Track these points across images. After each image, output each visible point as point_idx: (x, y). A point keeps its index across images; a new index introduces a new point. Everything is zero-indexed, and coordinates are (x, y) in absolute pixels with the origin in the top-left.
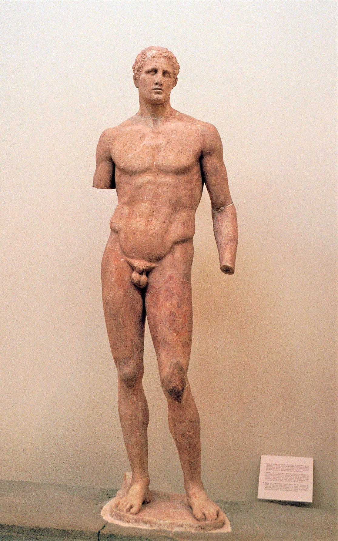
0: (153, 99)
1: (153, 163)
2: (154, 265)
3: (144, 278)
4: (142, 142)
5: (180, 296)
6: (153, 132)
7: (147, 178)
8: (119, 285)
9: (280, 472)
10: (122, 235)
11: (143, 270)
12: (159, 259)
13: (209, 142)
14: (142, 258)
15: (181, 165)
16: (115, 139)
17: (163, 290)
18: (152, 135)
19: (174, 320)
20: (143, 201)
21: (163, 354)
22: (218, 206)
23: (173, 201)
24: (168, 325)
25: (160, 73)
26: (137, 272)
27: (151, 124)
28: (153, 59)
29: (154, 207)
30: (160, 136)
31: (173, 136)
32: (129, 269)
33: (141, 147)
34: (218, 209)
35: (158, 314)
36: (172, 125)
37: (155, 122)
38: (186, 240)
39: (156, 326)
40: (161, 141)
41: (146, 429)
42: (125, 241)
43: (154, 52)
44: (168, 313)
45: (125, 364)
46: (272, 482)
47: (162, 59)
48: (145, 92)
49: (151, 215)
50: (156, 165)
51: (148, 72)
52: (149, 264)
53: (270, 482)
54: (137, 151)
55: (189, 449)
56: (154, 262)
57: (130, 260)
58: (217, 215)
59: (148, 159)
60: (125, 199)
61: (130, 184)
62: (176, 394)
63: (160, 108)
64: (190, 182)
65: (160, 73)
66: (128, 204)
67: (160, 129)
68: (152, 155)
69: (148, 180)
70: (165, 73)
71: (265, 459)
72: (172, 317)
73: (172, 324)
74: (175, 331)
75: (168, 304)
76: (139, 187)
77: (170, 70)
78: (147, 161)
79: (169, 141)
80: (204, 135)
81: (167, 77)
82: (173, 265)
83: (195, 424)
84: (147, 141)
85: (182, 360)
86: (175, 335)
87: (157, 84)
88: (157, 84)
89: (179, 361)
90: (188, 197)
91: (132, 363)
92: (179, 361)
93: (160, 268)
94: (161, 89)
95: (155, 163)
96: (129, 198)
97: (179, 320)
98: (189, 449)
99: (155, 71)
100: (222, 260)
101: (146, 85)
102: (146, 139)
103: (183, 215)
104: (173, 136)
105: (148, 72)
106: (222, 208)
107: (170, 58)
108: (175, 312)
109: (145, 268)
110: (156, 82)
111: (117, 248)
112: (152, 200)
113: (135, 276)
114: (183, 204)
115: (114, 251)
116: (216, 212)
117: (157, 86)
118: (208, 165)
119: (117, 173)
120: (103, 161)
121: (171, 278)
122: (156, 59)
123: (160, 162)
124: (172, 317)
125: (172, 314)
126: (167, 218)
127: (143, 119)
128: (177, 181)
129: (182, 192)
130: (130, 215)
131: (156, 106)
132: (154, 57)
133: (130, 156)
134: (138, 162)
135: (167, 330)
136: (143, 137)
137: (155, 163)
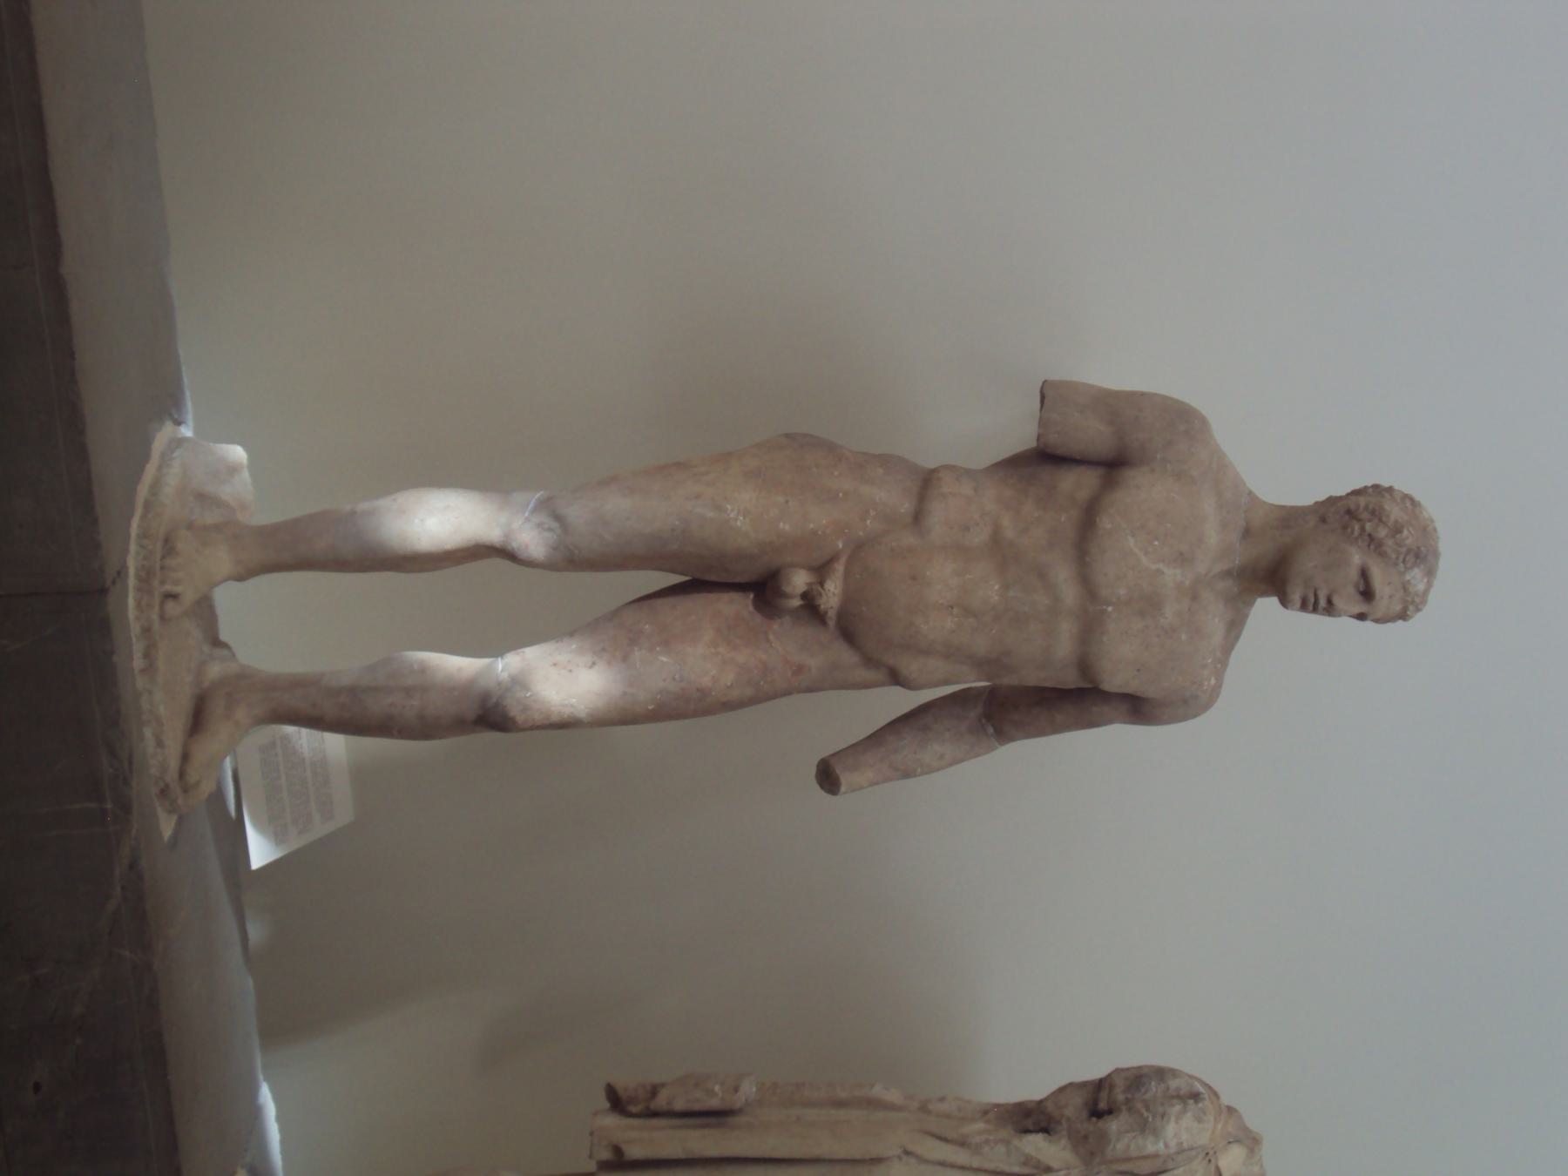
2: (832, 623)
3: (797, 602)
7: (1069, 593)
10: (909, 539)
12: (848, 634)
18: (1187, 583)
20: (1006, 587)
26: (810, 584)
27: (1218, 568)
31: (1184, 637)
33: (1154, 567)
36: (1214, 620)
37: (1227, 574)
40: (1170, 612)
49: (968, 611)
50: (1104, 612)
51: (1364, 574)
52: (832, 614)
54: (1144, 560)
57: (840, 567)
59: (1122, 592)
84: (1172, 575)
87: (1329, 602)
102: (1178, 572)
106: (991, 730)
107: (1403, 616)
110: (1336, 600)
133: (1131, 541)
136: (1183, 559)
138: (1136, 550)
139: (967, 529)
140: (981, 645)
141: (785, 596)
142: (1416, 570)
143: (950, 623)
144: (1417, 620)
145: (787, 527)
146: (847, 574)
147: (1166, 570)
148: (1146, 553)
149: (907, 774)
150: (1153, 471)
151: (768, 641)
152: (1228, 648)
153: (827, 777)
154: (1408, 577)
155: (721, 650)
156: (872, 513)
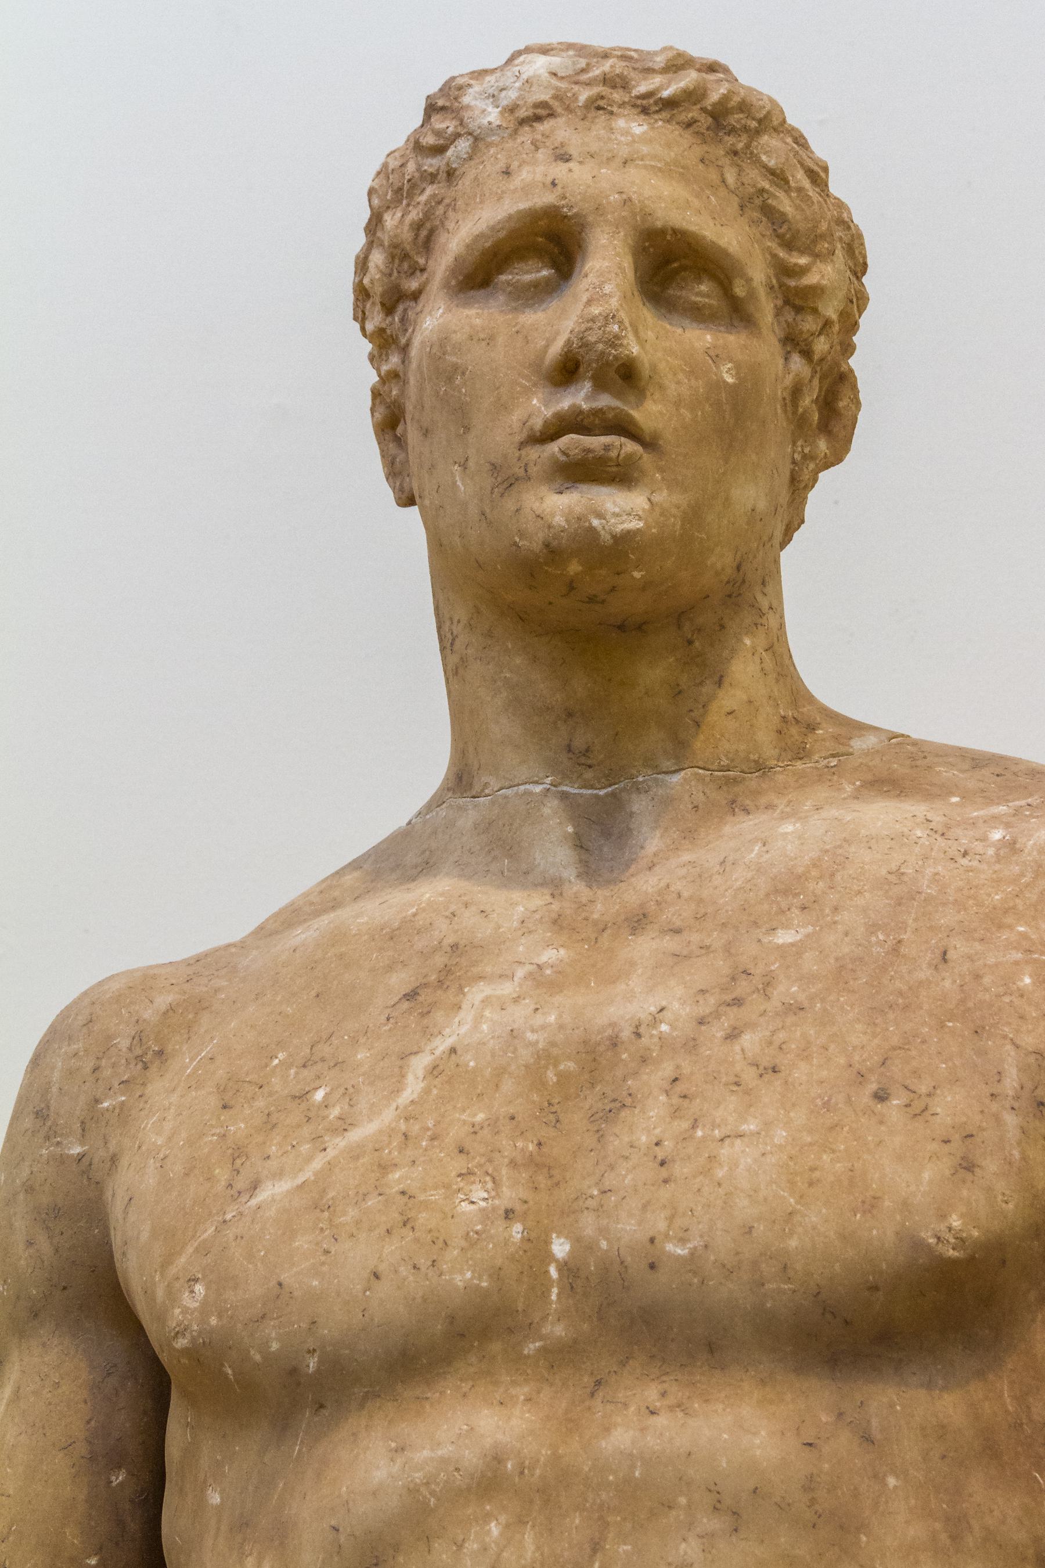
1: (537, 1248)
4: (429, 1033)
7: (475, 1424)
15: (882, 1232)
18: (549, 956)
25: (607, 267)
27: (553, 847)
28: (526, 135)
30: (645, 947)
31: (784, 937)
33: (413, 1087)
36: (788, 831)
40: (648, 995)
47: (638, 127)
50: (564, 1267)
51: (479, 276)
63: (653, 674)
65: (607, 267)
68: (540, 1166)
69: (471, 1458)
77: (729, 234)
78: (467, 1222)
79: (736, 992)
81: (698, 315)
87: (567, 371)
94: (624, 428)
95: (560, 1248)
99: (550, 244)
101: (461, 416)
102: (476, 994)
104: (784, 937)
105: (479, 276)
117: (579, 398)
122: (560, 130)
123: (628, 1228)
128: (844, 1442)
132: (542, 113)
133: (263, 1195)
134: (358, 1255)
137: (560, 1248)
147: (441, 1045)
148: (344, 1125)
154: (493, 116)
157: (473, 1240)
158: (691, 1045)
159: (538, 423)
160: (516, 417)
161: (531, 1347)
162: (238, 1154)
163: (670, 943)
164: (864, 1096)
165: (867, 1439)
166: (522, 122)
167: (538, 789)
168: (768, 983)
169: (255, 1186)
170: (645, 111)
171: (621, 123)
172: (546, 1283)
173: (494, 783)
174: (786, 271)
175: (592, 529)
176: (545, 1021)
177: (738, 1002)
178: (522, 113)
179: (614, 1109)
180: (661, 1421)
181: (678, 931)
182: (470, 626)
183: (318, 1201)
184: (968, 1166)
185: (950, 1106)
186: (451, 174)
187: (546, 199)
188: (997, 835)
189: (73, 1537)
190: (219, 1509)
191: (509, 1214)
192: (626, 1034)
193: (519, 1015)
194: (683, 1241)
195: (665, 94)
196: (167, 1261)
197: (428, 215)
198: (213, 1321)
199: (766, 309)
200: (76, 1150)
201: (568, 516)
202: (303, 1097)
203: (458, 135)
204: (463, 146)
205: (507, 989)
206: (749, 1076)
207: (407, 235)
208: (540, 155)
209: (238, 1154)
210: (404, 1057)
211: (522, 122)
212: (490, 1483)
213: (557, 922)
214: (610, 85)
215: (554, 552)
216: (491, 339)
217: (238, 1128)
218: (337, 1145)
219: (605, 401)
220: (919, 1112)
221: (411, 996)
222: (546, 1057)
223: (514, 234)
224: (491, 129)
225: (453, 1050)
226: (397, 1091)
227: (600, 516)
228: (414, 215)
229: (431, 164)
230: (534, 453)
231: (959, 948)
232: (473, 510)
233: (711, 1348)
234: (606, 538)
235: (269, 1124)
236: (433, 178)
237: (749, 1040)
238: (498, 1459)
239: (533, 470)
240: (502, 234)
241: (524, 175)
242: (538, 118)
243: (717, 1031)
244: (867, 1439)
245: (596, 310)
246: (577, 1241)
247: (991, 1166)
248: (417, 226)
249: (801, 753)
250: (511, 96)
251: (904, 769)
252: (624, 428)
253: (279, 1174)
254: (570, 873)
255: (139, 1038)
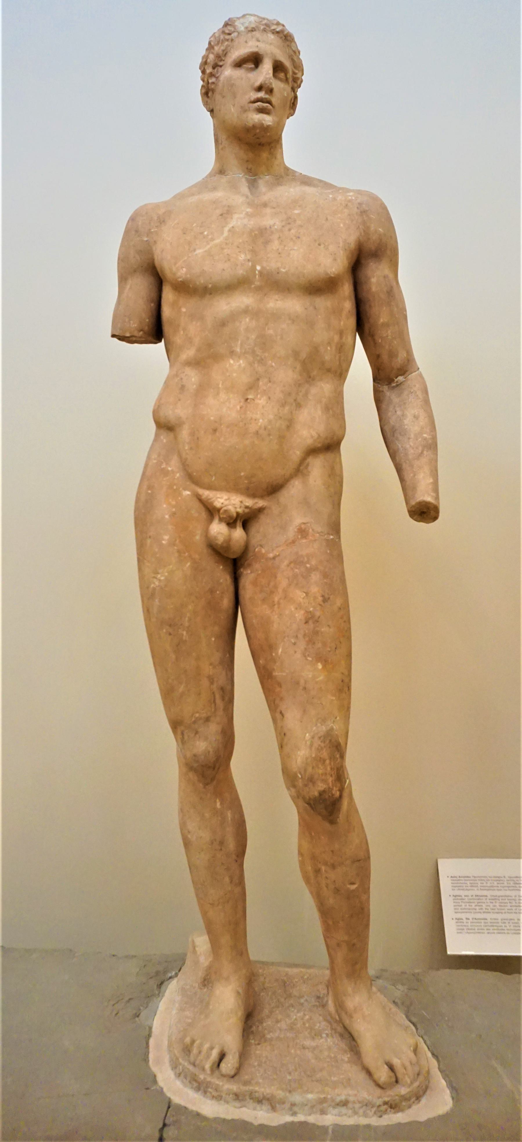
0: (250, 124)
1: (253, 268)
2: (261, 503)
3: (238, 533)
5: (325, 575)
6: (250, 204)
8: (179, 551)
9: (479, 893)
10: (184, 433)
11: (238, 514)
12: (273, 489)
13: (377, 229)
14: (234, 488)
15: (321, 270)
16: (162, 221)
17: (286, 563)
18: (249, 210)
19: (316, 633)
20: (232, 353)
21: (292, 718)
22: (389, 375)
23: (303, 355)
24: (302, 644)
25: (267, 67)
26: (221, 520)
27: (244, 188)
28: (250, 35)
29: (260, 369)
30: (268, 211)
31: (296, 212)
32: (204, 515)
33: (226, 234)
34: (390, 381)
35: (275, 618)
37: (253, 184)
38: (330, 446)
39: (272, 647)
41: (241, 865)
42: (191, 449)
43: (252, 19)
44: (300, 615)
45: (197, 733)
46: (468, 915)
47: (272, 36)
48: (232, 112)
50: (259, 271)
51: (239, 64)
52: (249, 502)
53: (463, 916)
54: (217, 241)
55: (346, 916)
56: (262, 497)
57: (206, 494)
58: (388, 394)
59: (242, 257)
60: (189, 353)
61: (202, 318)
62: (325, 807)
63: (265, 155)
64: (337, 312)
65: (267, 67)
66: (196, 363)
67: (265, 198)
68: (253, 251)
69: (243, 306)
70: (278, 67)
71: (449, 869)
72: (311, 625)
73: (311, 642)
74: (319, 658)
75: (299, 595)
76: (223, 323)
77: (287, 64)
79: (289, 221)
80: (363, 212)
81: (281, 80)
82: (305, 502)
83: (362, 863)
84: (237, 221)
85: (337, 727)
86: (320, 666)
87: (260, 89)
88: (260, 89)
89: (332, 729)
90: (334, 348)
91: (213, 728)
92: (332, 729)
93: (275, 510)
94: (269, 102)
95: (258, 268)
96: (199, 350)
97: (327, 630)
98: (346, 916)
99: (255, 60)
100: (414, 488)
102: (236, 216)
103: (325, 387)
104: (296, 212)
105: (239, 64)
106: (401, 378)
107: (287, 38)
108: (318, 614)
109: (240, 510)
110: (257, 84)
111: (173, 465)
112: (253, 352)
113: (218, 529)
114: (323, 363)
115: (165, 473)
116: (385, 388)
117: (261, 95)
118: (374, 280)
119: (168, 295)
120: (135, 271)
121: (302, 532)
122: (257, 34)
124: (311, 625)
125: (310, 618)
126: (290, 394)
127: (224, 179)
129: (321, 334)
130: (202, 389)
131: (253, 146)
132: (253, 30)
133: (198, 251)
134: (220, 266)
135: (298, 655)
136: (227, 213)
137: (258, 268)
138: (208, 247)
139: (183, 387)
140: (286, 375)
141: (228, 540)
142: (236, 24)
143: (262, 401)
144: (290, 28)
145: (166, 537)
146: (210, 488)
147: (230, 226)
148: (212, 239)
149: (432, 446)
150: (155, 242)
151: (274, 558)
152: (327, 185)
153: (425, 513)
154: (242, 29)
155: (276, 599)
156: (164, 466)
157: (242, 265)
158: (281, 231)
159: (252, 99)
160: (247, 97)
161: (253, 286)
162: (189, 243)
163: (273, 210)
164: (317, 244)
165: (315, 308)
166: (249, 31)
167: (241, 176)
168: (295, 221)
169: (195, 250)
170: (273, 33)
171: (269, 35)
172: (255, 275)
173: (231, 173)
174: (294, 73)
175: (263, 124)
176: (251, 223)
177: (289, 224)
178: (250, 29)
179: (267, 242)
180: (279, 302)
181: (274, 208)
182: (226, 139)
183: (209, 254)
184: (335, 260)
185: (332, 248)
186: (232, 40)
187: (255, 50)
188: (331, 196)
189: (144, 316)
190: (185, 312)
191: (249, 260)
192: (268, 227)
193: (245, 221)
194: (284, 269)
195: (278, 30)
196: (175, 264)
197: (226, 49)
198: (188, 276)
199: (290, 80)
200: (146, 239)
201: (259, 120)
202: (202, 233)
203: (234, 32)
204: (235, 34)
205: (242, 216)
206: (294, 238)
207: (221, 52)
208: (254, 39)
209: (189, 243)
210: (223, 227)
211: (249, 31)
212: (246, 311)
213: (249, 204)
214: (267, 27)
215: (254, 127)
216: (242, 79)
217: (188, 238)
218: (212, 244)
219: (267, 96)
220: (326, 248)
221: (222, 215)
222: (252, 231)
223: (249, 56)
224: (242, 31)
225: (233, 227)
226: (222, 233)
227: (264, 120)
228: (222, 48)
229: (227, 37)
230: (251, 105)
231: (329, 218)
232: (236, 115)
233: (288, 289)
234: (265, 126)
235: (195, 238)
236: (228, 40)
237: (293, 231)
238: (247, 306)
239: (251, 109)
240: (246, 56)
241: (250, 43)
242: (252, 31)
243: (286, 228)
244: (315, 308)
245: (268, 76)
246: (262, 267)
247: (339, 261)
248: (223, 51)
249: (288, 175)
250: (247, 25)
251: (306, 181)
252: (269, 102)
253: (200, 248)
254: (249, 194)
255: (159, 217)
